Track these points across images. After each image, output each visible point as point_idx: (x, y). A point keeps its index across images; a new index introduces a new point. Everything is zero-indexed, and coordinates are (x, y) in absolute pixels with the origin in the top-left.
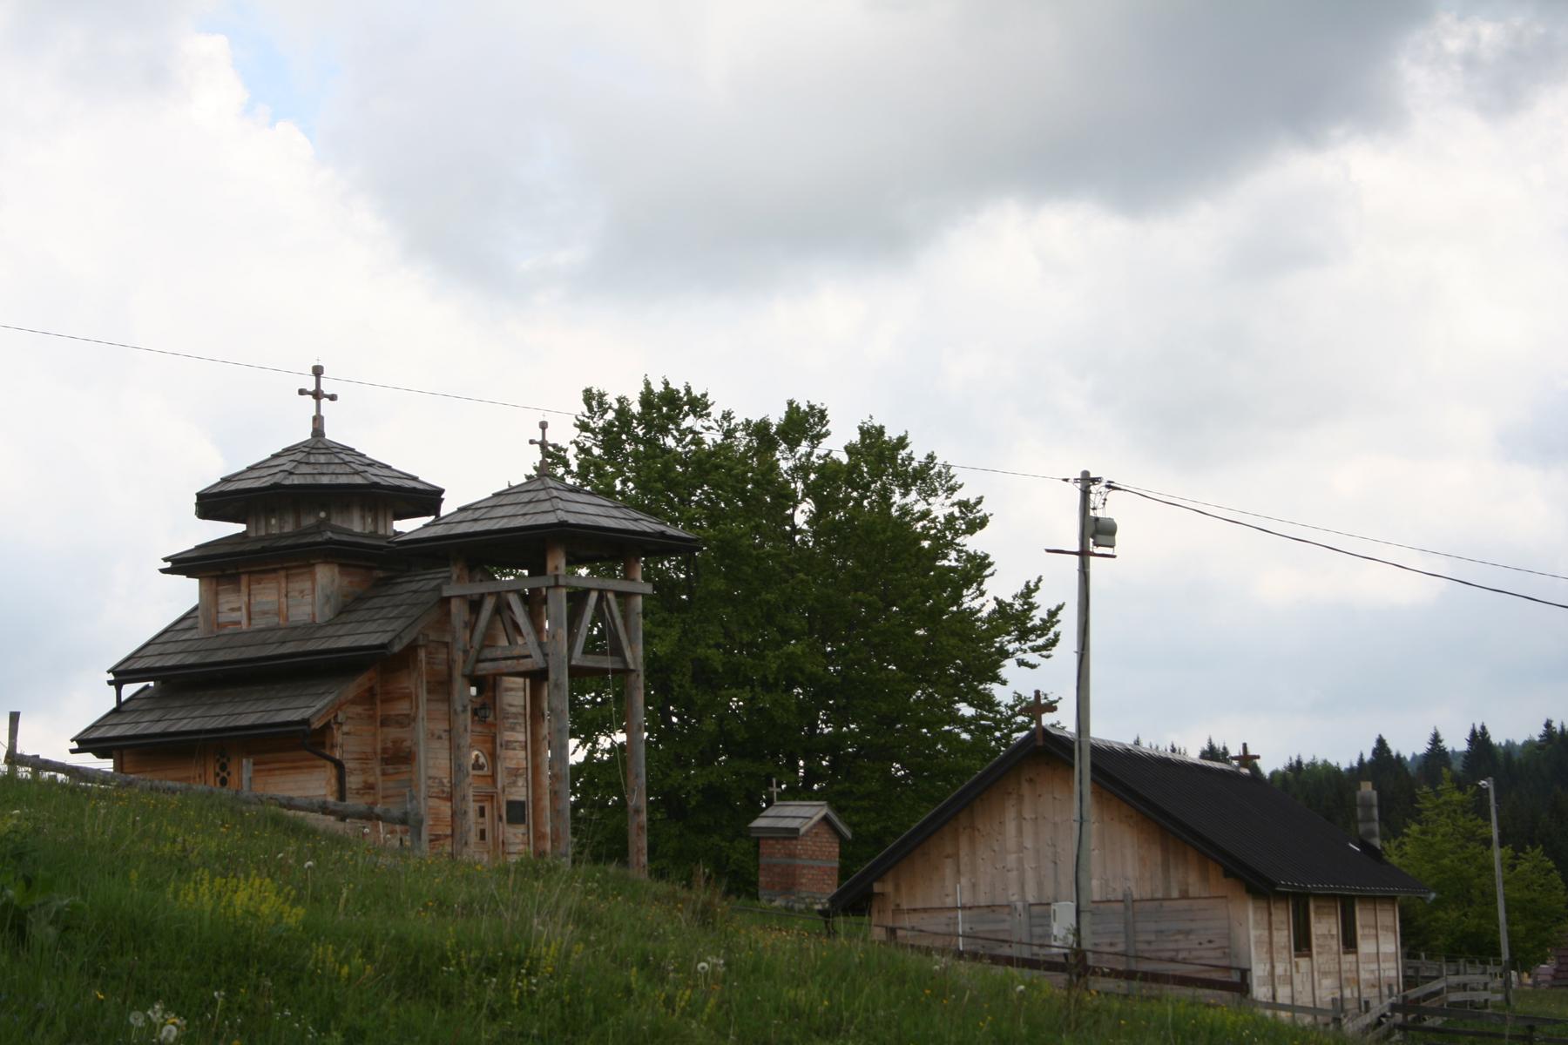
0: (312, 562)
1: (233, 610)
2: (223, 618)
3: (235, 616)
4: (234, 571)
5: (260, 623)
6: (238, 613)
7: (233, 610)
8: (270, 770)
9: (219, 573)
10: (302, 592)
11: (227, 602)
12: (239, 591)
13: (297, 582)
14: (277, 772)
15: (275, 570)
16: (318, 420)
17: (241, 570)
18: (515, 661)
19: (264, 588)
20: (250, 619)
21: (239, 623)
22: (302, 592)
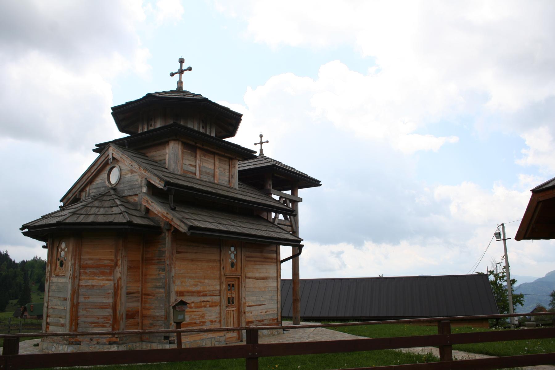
0: (237, 158)
1: (191, 165)
2: (185, 168)
3: (192, 169)
4: (201, 146)
5: (205, 178)
6: (194, 169)
7: (191, 165)
8: (255, 261)
9: (193, 143)
10: (225, 169)
11: (188, 160)
12: (196, 157)
13: (223, 164)
14: (258, 263)
15: (214, 154)
16: (180, 83)
17: (205, 147)
18: (287, 227)
19: (207, 160)
20: (200, 174)
21: (195, 174)
22: (225, 169)
